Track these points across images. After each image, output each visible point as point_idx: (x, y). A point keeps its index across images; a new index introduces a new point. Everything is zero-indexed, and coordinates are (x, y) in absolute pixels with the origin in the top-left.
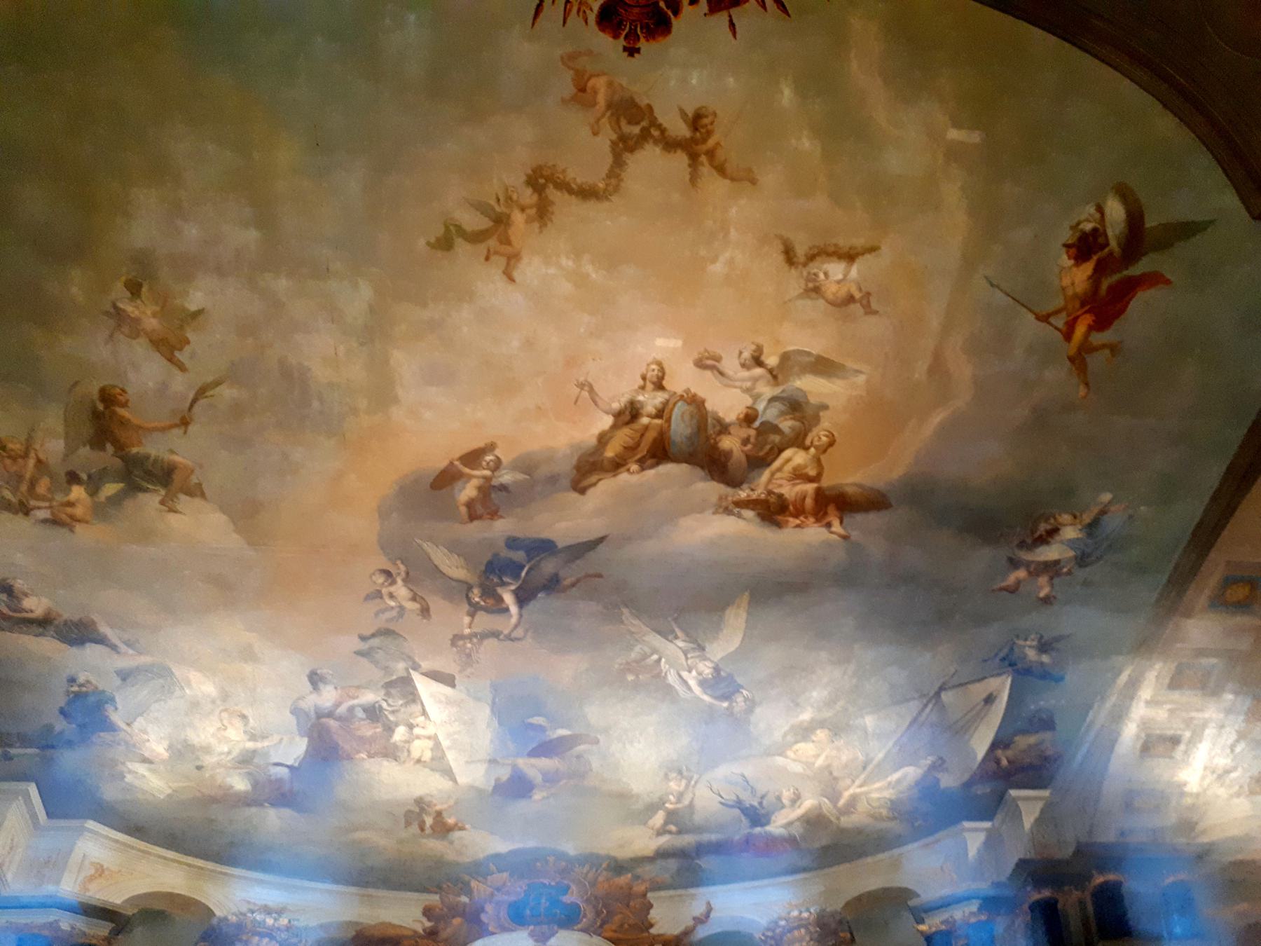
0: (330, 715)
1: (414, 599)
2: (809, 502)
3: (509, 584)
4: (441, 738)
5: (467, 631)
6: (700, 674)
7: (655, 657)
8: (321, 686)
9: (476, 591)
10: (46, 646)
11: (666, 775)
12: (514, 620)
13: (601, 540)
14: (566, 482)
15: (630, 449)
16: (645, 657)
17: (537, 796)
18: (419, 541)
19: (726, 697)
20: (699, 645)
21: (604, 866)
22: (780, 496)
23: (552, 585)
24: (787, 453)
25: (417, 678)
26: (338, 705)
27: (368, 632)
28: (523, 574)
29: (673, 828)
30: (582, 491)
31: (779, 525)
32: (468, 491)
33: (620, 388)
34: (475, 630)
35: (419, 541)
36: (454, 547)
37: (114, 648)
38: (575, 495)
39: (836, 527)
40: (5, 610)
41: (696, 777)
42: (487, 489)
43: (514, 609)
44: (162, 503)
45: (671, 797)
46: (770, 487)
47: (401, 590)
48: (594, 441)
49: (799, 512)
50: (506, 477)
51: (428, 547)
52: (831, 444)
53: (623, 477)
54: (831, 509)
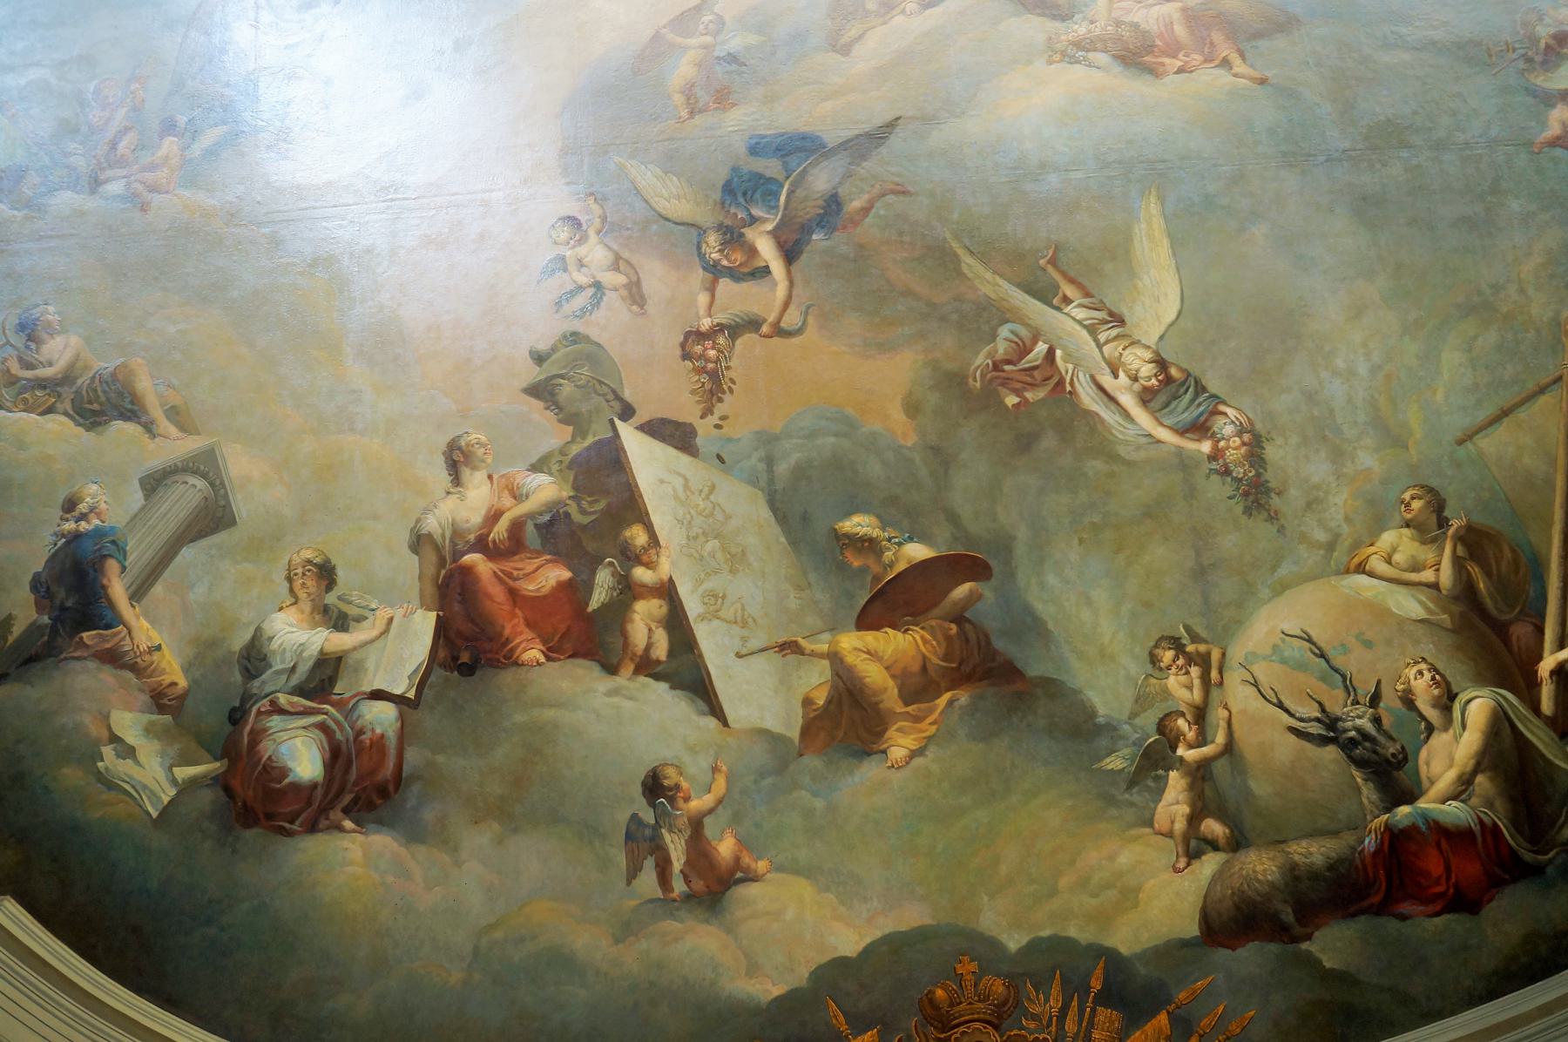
0: (482, 544)
1: (615, 267)
2: (1180, 31)
3: (765, 221)
4: (683, 590)
5: (706, 324)
6: (1135, 379)
7: (1041, 348)
8: (466, 473)
10: (55, 433)
11: (1154, 660)
12: (781, 291)
13: (891, 126)
16: (1024, 350)
17: (900, 744)
19: (1199, 428)
20: (1111, 314)
21: (1096, 985)
22: (1136, 26)
25: (633, 441)
26: (494, 517)
27: (542, 346)
28: (783, 198)
29: (1213, 827)
30: (846, 50)
31: (1153, 72)
32: (682, 70)
34: (721, 318)
37: (149, 427)
39: (1239, 66)
40: (15, 369)
41: (1215, 656)
43: (777, 267)
45: (1181, 722)
46: (1115, 14)
49: (1173, 50)
50: (735, 42)
53: (899, 19)
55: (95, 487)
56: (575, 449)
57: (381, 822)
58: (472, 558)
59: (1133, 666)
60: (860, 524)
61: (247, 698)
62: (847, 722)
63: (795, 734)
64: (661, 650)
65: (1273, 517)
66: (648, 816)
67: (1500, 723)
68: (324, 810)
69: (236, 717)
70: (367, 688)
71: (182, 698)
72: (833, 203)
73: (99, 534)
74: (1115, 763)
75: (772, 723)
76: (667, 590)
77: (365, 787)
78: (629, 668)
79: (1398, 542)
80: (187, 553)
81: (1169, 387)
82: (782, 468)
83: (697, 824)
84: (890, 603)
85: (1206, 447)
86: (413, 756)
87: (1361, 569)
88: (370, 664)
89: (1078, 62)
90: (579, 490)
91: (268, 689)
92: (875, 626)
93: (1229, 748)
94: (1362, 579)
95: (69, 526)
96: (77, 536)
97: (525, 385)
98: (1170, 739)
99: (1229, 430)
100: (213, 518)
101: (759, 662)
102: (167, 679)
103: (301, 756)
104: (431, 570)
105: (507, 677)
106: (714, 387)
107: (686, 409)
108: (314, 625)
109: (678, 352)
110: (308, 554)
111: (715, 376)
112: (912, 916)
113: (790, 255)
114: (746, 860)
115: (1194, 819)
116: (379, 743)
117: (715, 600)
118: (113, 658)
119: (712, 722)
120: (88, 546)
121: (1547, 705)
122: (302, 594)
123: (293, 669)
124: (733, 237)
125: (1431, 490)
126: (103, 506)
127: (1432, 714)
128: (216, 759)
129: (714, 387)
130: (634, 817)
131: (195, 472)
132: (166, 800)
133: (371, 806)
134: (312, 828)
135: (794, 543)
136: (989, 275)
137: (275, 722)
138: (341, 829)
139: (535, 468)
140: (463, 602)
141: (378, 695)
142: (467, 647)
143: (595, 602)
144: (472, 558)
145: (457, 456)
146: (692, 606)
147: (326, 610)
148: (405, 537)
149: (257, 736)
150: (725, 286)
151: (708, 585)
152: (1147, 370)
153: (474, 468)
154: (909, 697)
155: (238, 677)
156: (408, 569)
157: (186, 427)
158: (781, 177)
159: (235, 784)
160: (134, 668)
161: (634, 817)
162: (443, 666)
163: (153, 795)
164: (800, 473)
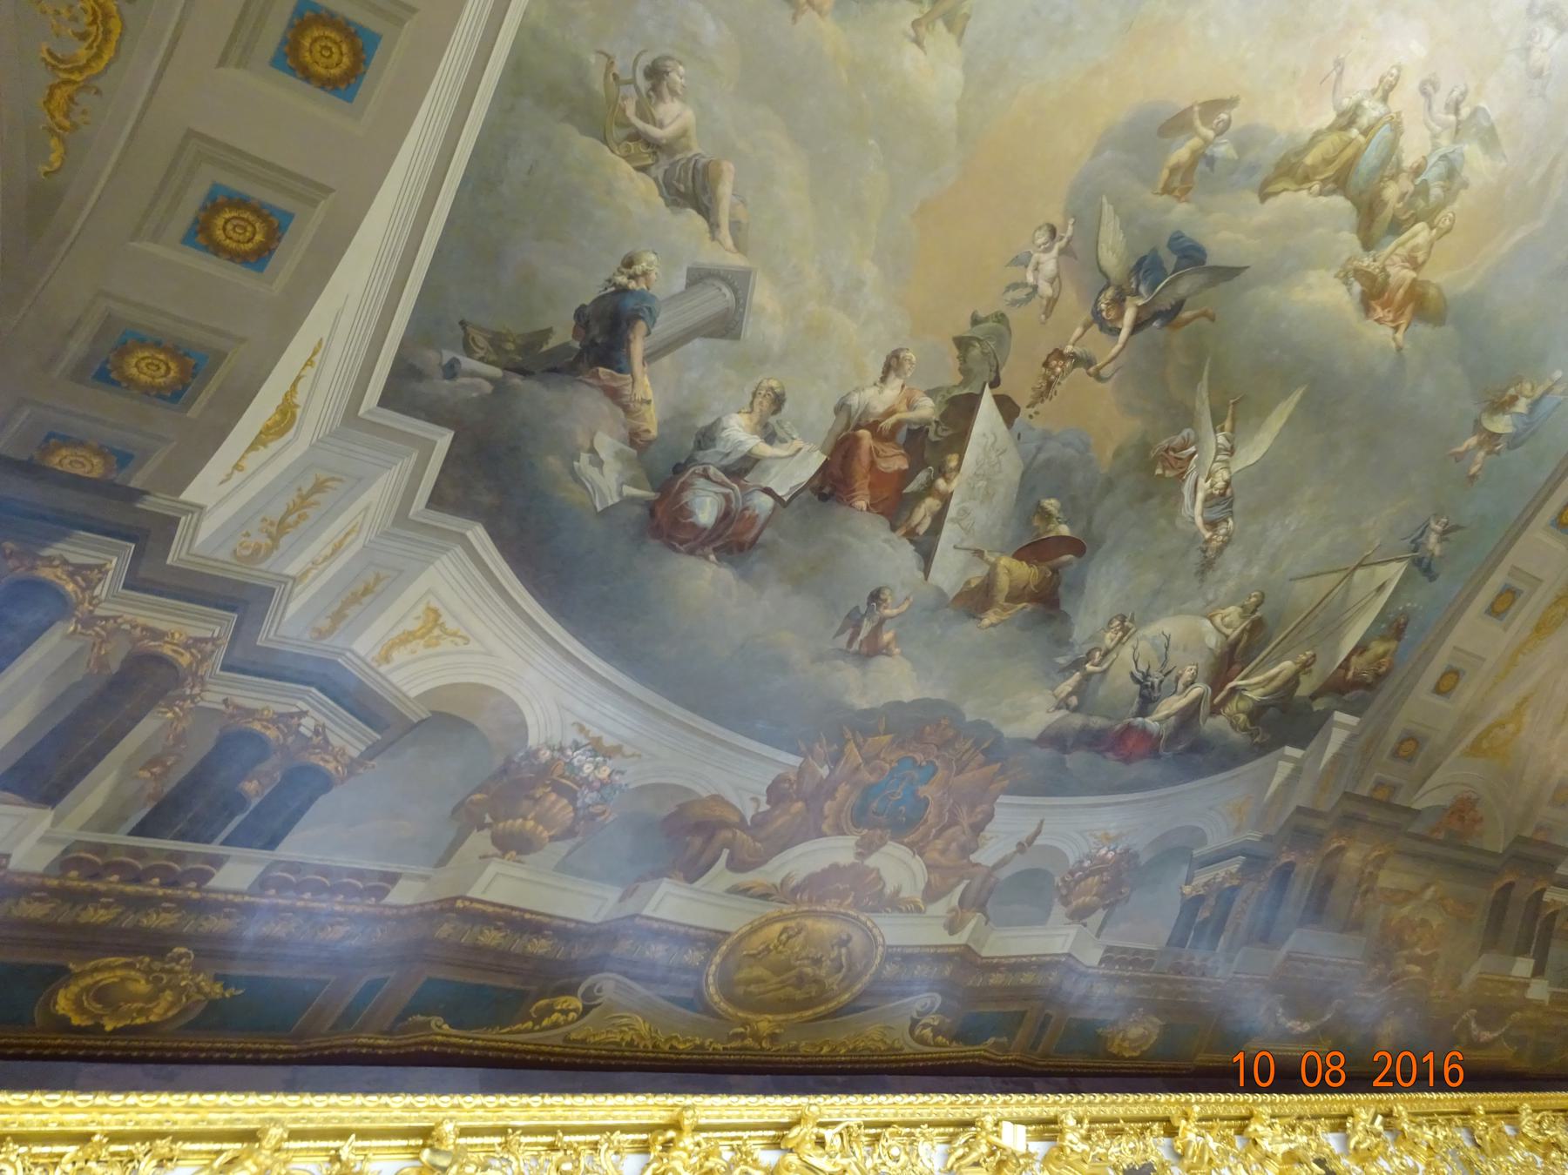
0: (873, 427)
1: (1051, 282)
5: (1069, 349)
6: (1212, 486)
7: (1193, 449)
8: (892, 375)
9: (1110, 293)
10: (637, 191)
14: (1258, 178)
15: (1328, 162)
17: (990, 618)
18: (1104, 200)
23: (1170, 315)
24: (1419, 226)
25: (987, 405)
26: (890, 413)
27: (982, 314)
30: (1264, 197)
32: (1181, 154)
33: (1359, 84)
34: (1078, 350)
35: (1104, 200)
36: (1127, 222)
37: (714, 226)
38: (1255, 199)
42: (1199, 156)
44: (916, 24)
47: (1049, 263)
48: (1307, 137)
50: (1224, 149)
51: (1108, 209)
52: (1448, 231)
54: (1410, 308)
55: (653, 257)
56: (956, 392)
57: (731, 563)
58: (865, 434)
59: (1100, 621)
60: (1051, 504)
61: (691, 460)
62: (977, 599)
63: (951, 597)
64: (922, 530)
65: (1202, 581)
66: (863, 610)
67: (1200, 698)
68: (703, 544)
69: (679, 469)
70: (764, 485)
71: (650, 442)
72: (1179, 306)
73: (642, 296)
74: (1062, 661)
75: (946, 587)
76: (946, 499)
77: (733, 540)
78: (902, 531)
79: (1233, 612)
80: (697, 344)
81: (1221, 501)
82: (1042, 457)
83: (882, 621)
84: (1035, 550)
85: (1208, 535)
86: (767, 534)
87: (1211, 619)
88: (773, 471)
89: (1346, 283)
90: (944, 416)
91: (706, 460)
92: (1020, 559)
93: (1105, 672)
94: (1208, 623)
95: (622, 280)
96: (622, 291)
97: (957, 334)
98: (1089, 657)
99: (1223, 531)
100: (726, 326)
101: (962, 555)
102: (645, 426)
103: (705, 509)
104: (839, 429)
105: (841, 511)
106: (1046, 390)
107: (1022, 398)
108: (754, 432)
109: (1044, 358)
110: (774, 383)
111: (1050, 384)
112: (941, 694)
113: (1138, 326)
114: (892, 646)
115: (1070, 694)
116: (754, 518)
117: (964, 512)
118: (614, 394)
119: (921, 575)
120: (630, 303)
121: (1217, 700)
122: (757, 409)
123: (727, 455)
124: (1119, 302)
125: (1263, 595)
126: (653, 276)
127: (1180, 686)
128: (654, 490)
129: (1046, 390)
130: (857, 608)
131: (730, 285)
132: (610, 503)
133: (730, 551)
134: (691, 552)
135: (1018, 500)
136: (1205, 395)
137: (701, 482)
138: (707, 558)
139: (929, 393)
140: (845, 457)
141: (768, 491)
142: (831, 485)
143: (908, 489)
144: (865, 434)
145: (894, 362)
146: (952, 512)
147: (766, 426)
148: (836, 401)
149: (685, 486)
150: (1095, 327)
151: (966, 504)
152: (1221, 484)
153: (898, 376)
154: (1008, 599)
155: (691, 445)
156: (825, 422)
157: (739, 247)
158: (1170, 270)
159: (659, 510)
160: (626, 409)
161: (857, 608)
162: (813, 489)
163: (603, 497)
164: (1048, 463)
